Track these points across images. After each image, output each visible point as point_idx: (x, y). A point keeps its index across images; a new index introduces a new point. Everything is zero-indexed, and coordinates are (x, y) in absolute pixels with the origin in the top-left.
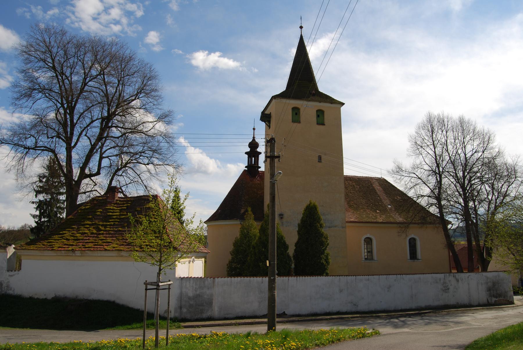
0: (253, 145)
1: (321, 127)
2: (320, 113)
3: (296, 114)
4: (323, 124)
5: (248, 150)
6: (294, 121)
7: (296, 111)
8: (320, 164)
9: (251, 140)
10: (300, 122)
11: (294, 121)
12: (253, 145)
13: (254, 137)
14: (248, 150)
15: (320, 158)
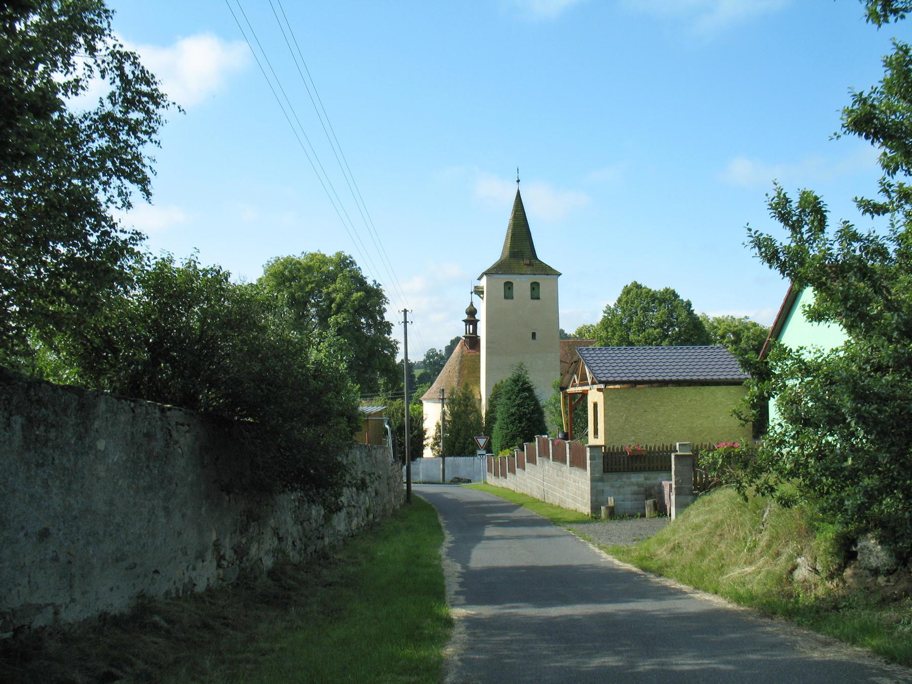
0: (472, 312)
1: (536, 301)
2: (535, 286)
3: (509, 288)
4: (538, 298)
5: (466, 317)
6: (506, 297)
7: (509, 286)
8: (534, 341)
9: (468, 305)
10: (512, 298)
11: (506, 297)
12: (472, 312)
13: (472, 303)
14: (466, 317)
15: (534, 335)
